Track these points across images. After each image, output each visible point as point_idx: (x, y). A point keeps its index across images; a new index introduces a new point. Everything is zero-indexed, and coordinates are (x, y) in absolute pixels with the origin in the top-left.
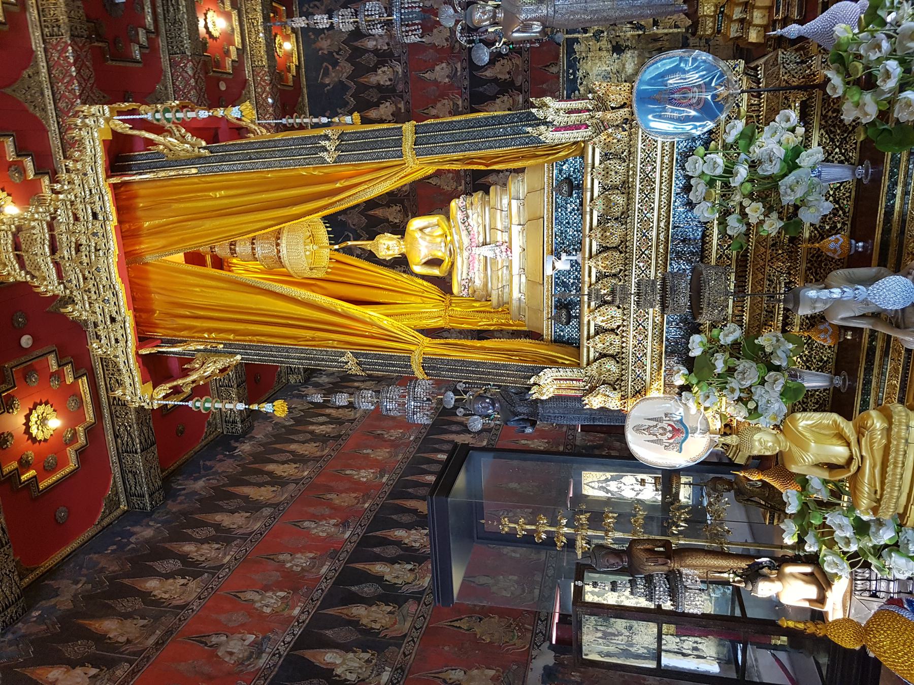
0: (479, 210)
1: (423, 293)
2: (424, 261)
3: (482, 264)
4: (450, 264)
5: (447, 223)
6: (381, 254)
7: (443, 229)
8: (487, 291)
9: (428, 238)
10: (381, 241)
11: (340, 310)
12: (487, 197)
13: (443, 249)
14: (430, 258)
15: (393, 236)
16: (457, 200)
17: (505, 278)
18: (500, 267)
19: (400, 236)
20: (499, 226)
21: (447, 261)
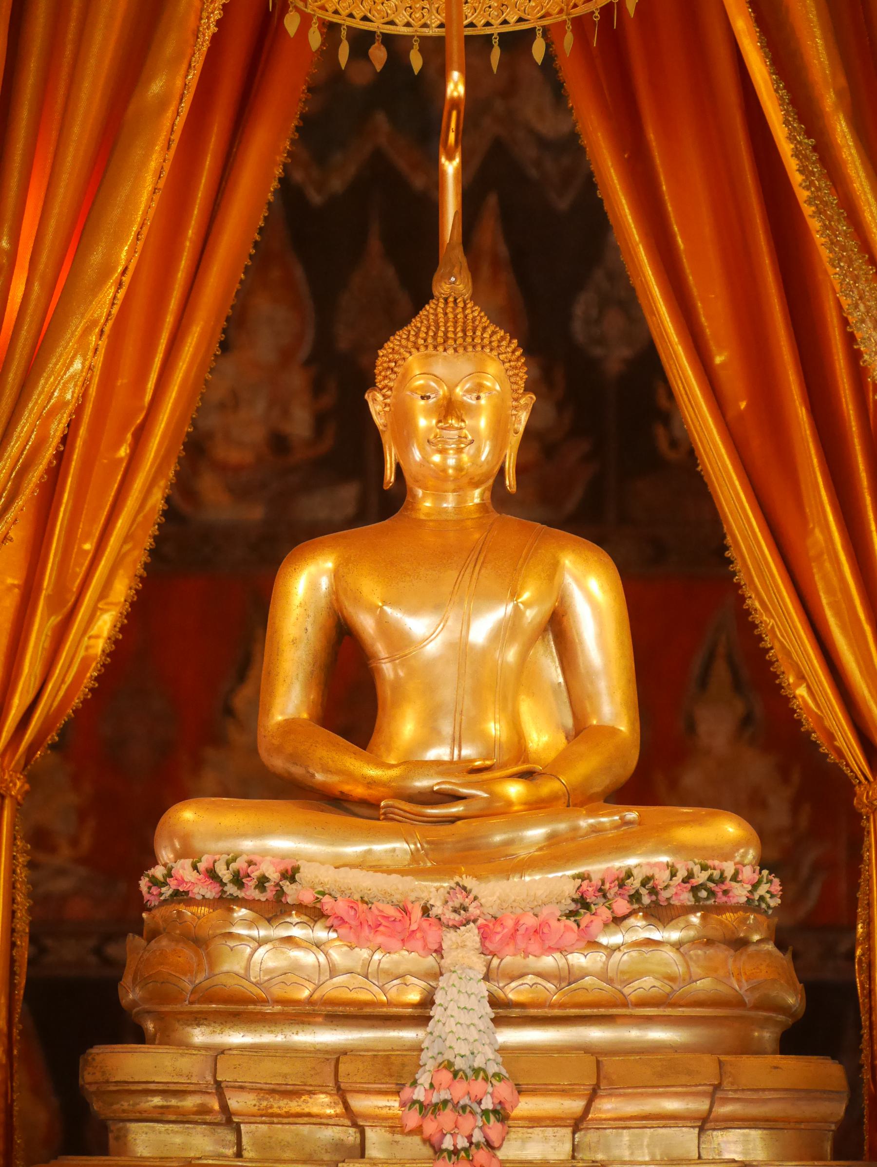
0: (704, 985)
1: (54, 605)
2: (366, 624)
3: (368, 993)
4: (359, 791)
5: (601, 784)
6: (414, 362)
7: (563, 760)
8: (199, 1019)
9: (511, 655)
10: (493, 368)
11: (156, 87)
12: (767, 1035)
13: (440, 752)
14: (387, 669)
15: (515, 440)
16: (751, 855)
17: (284, 1132)
18: (361, 1103)
19: (510, 481)
20: (607, 1106)
21: (373, 772)
